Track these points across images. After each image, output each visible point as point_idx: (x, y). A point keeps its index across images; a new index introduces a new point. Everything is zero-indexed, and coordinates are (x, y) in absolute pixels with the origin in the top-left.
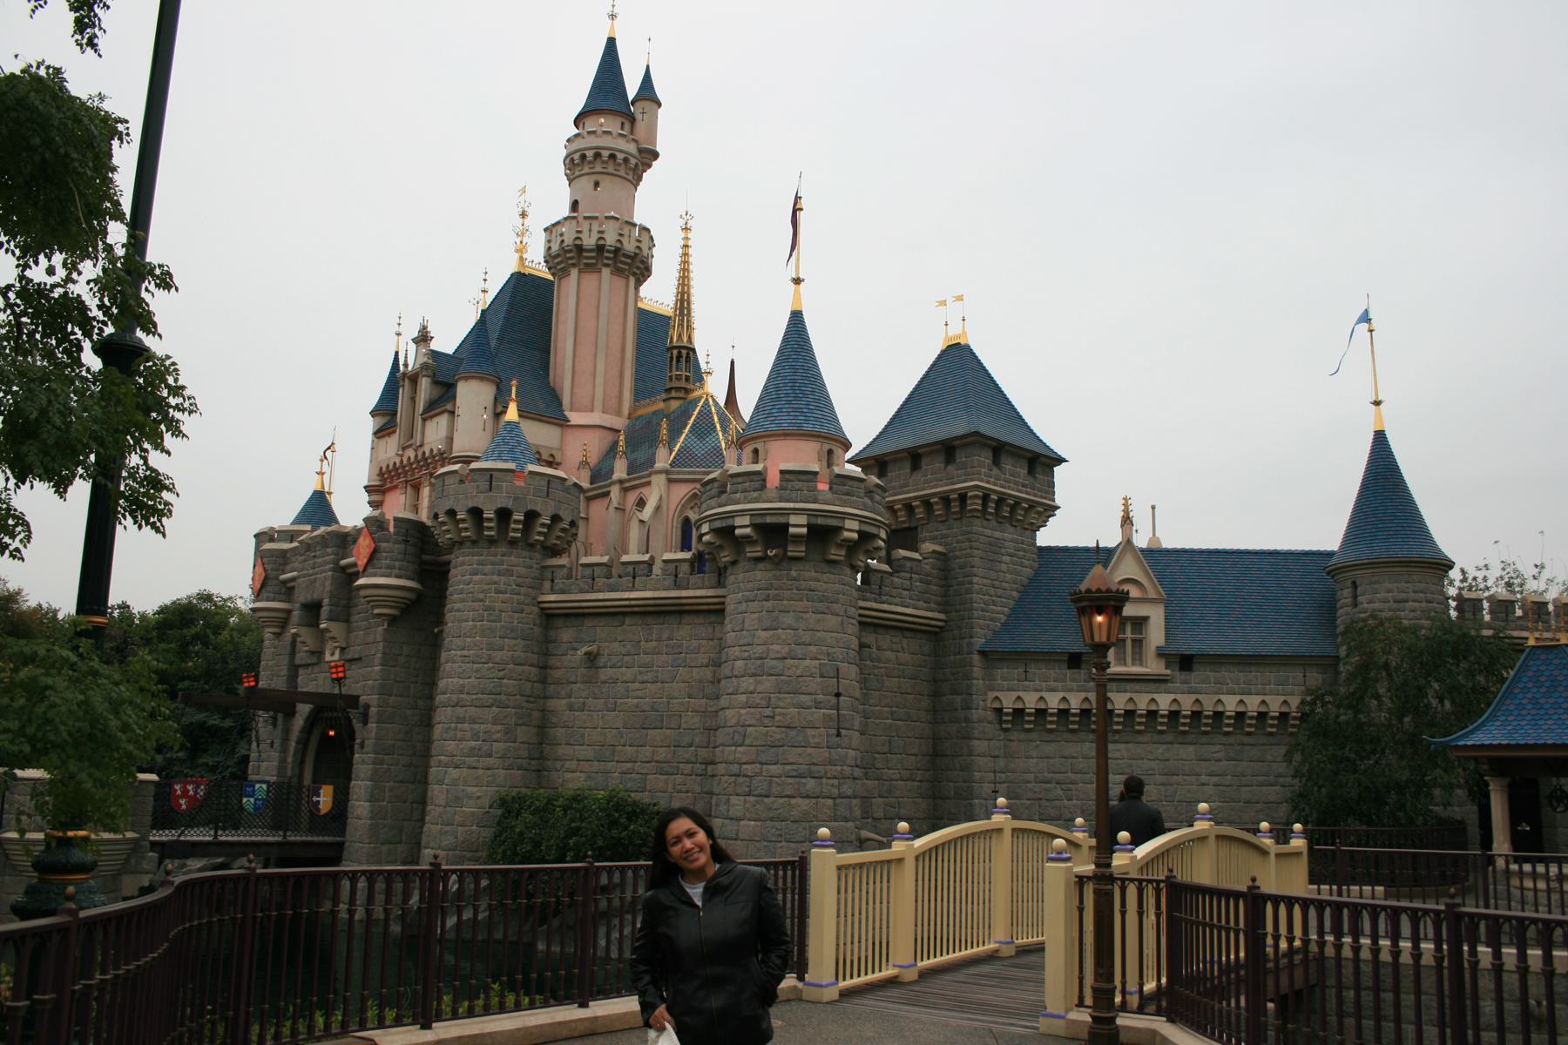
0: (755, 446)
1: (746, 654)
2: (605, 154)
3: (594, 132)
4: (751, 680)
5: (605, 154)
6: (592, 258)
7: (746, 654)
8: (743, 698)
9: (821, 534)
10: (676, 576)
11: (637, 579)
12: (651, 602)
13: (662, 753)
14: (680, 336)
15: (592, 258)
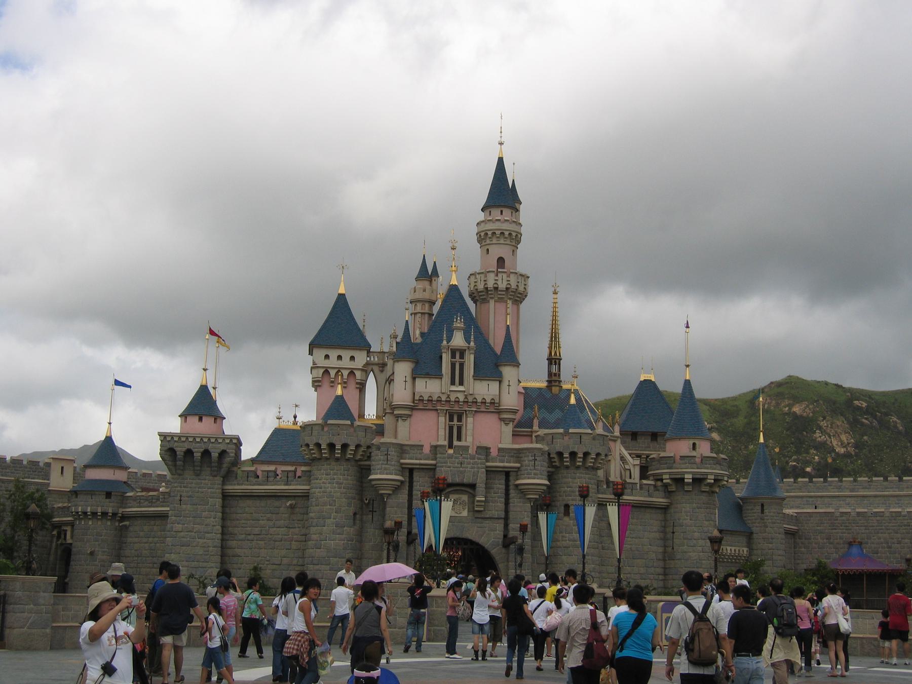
0: (695, 441)
1: (700, 531)
2: (498, 232)
3: (508, 220)
4: (703, 541)
5: (498, 232)
6: (504, 295)
7: (700, 531)
8: (700, 549)
9: (698, 481)
10: (648, 491)
11: (633, 490)
12: (641, 502)
13: (642, 570)
14: (556, 353)
15: (504, 295)
